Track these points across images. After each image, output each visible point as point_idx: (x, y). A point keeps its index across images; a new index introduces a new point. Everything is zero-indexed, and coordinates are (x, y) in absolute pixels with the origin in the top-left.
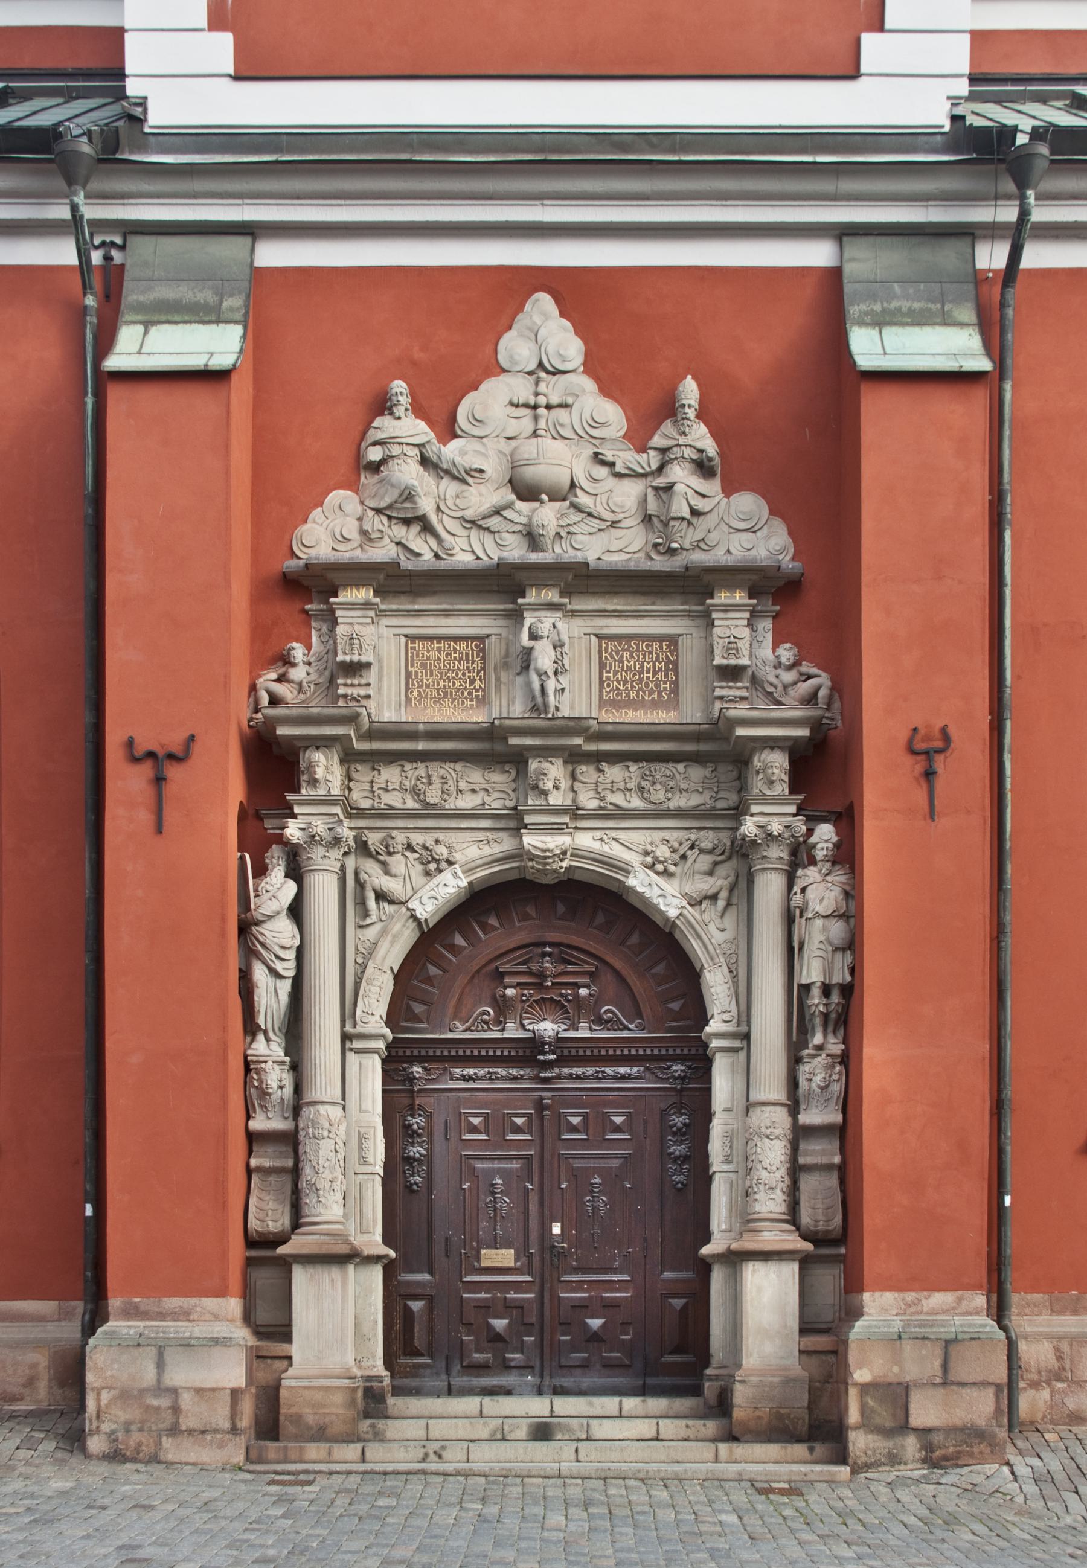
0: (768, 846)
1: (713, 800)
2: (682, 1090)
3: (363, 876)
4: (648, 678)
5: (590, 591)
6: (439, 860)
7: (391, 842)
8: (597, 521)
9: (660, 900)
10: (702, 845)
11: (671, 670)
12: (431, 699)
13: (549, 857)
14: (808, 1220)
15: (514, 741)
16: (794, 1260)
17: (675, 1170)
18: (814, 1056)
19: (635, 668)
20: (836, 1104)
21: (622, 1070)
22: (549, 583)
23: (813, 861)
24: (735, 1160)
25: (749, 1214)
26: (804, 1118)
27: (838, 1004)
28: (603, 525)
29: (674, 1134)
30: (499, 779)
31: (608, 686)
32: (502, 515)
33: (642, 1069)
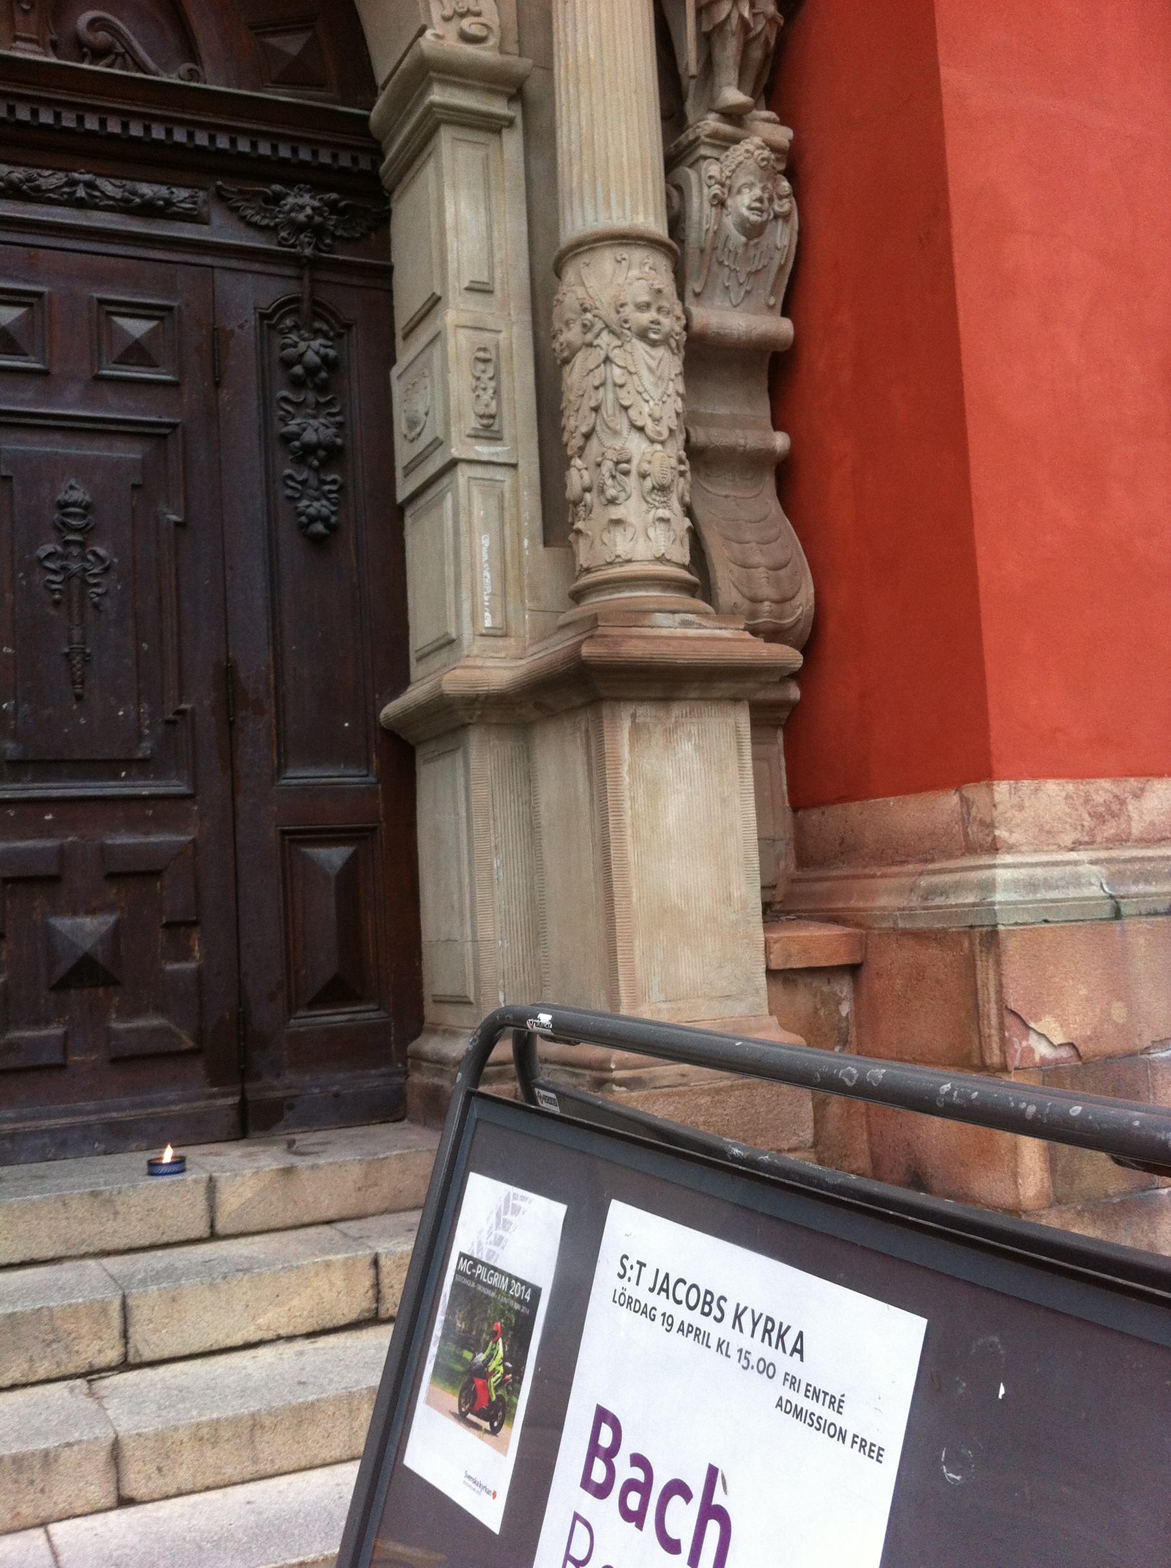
2: (314, 264)
16: (735, 700)
17: (303, 483)
18: (725, 142)
20: (773, 293)
21: (147, 190)
24: (507, 434)
27: (771, 20)
29: (297, 383)
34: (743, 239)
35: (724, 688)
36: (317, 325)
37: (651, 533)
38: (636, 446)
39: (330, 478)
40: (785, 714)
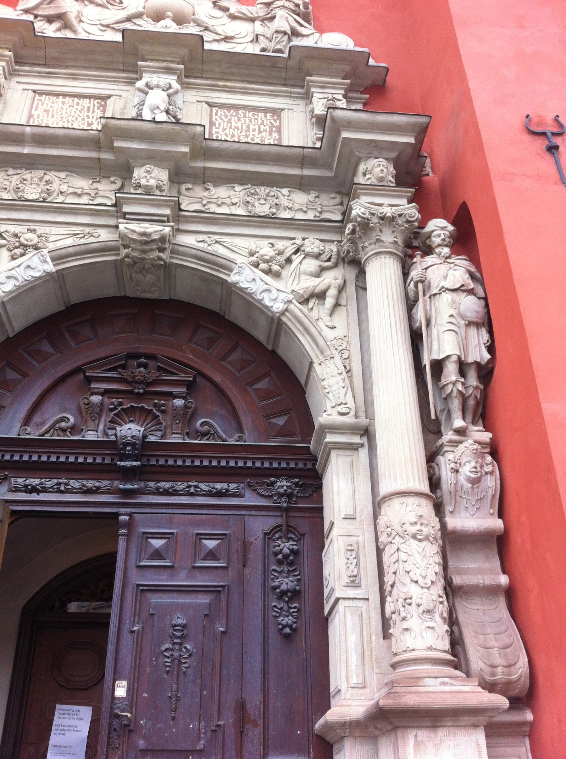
0: (381, 231)
2: (288, 509)
5: (204, 76)
8: (214, 35)
9: (265, 296)
10: (308, 250)
11: (275, 132)
14: (481, 665)
16: (475, 726)
17: (281, 609)
18: (456, 444)
19: (242, 128)
20: (491, 507)
21: (218, 486)
22: (168, 59)
23: (428, 251)
24: (363, 584)
25: (396, 654)
26: (453, 522)
27: (476, 388)
28: (218, 37)
29: (280, 562)
32: (133, 22)
33: (242, 485)
34: (470, 485)
35: (466, 720)
36: (290, 536)
37: (424, 634)
38: (414, 591)
39: (293, 606)
40: (528, 729)
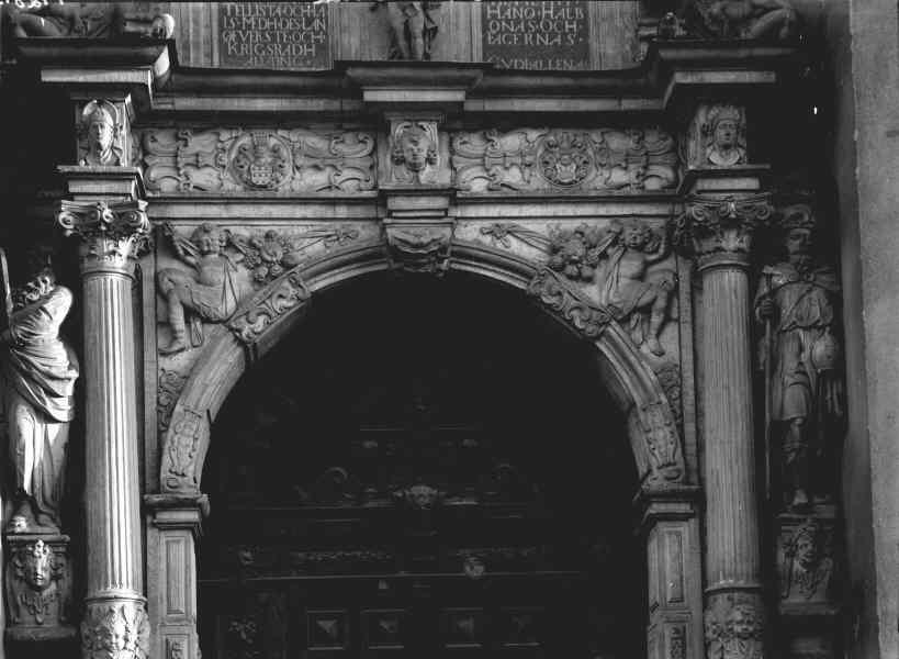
1: (641, 178)
3: (166, 285)
4: (548, 16)
6: (272, 262)
7: (205, 237)
12: (254, 44)
13: (423, 256)
15: (369, 96)
30: (354, 149)
31: (495, 27)
